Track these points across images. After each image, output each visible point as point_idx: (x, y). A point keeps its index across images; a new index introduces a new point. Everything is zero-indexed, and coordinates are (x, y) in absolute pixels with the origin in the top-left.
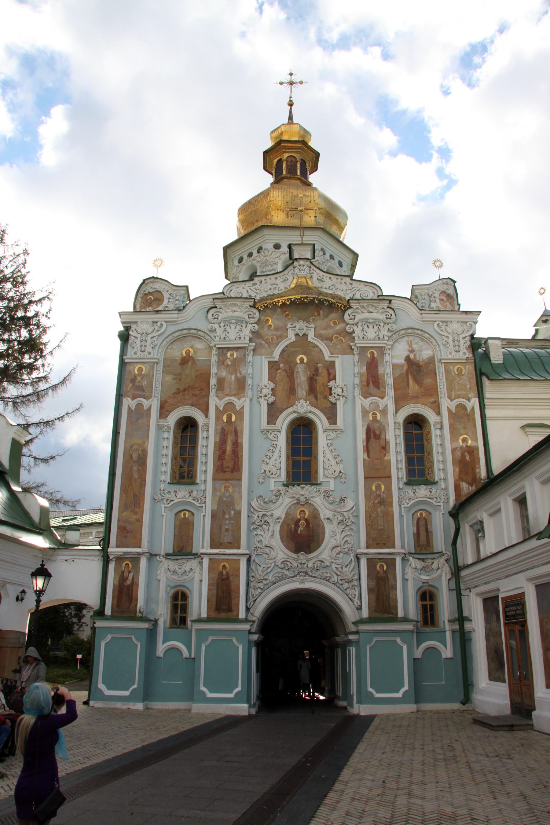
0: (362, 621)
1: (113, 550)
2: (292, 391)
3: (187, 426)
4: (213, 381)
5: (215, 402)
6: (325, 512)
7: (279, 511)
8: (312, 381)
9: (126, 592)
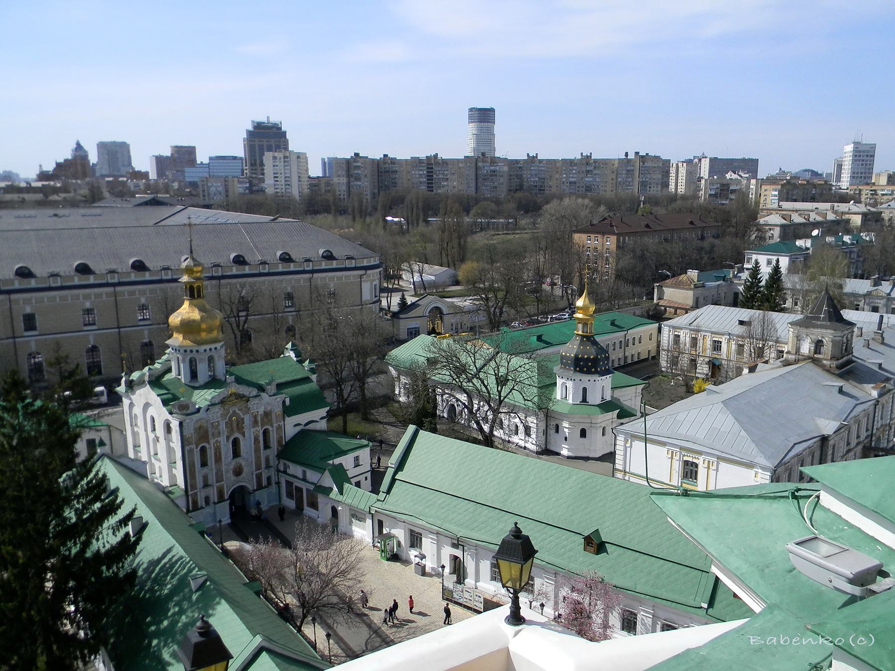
0: (254, 491)
1: (190, 493)
2: (232, 430)
3: (203, 450)
4: (210, 433)
5: (212, 441)
6: (243, 464)
7: (232, 467)
8: (237, 425)
9: (195, 503)
